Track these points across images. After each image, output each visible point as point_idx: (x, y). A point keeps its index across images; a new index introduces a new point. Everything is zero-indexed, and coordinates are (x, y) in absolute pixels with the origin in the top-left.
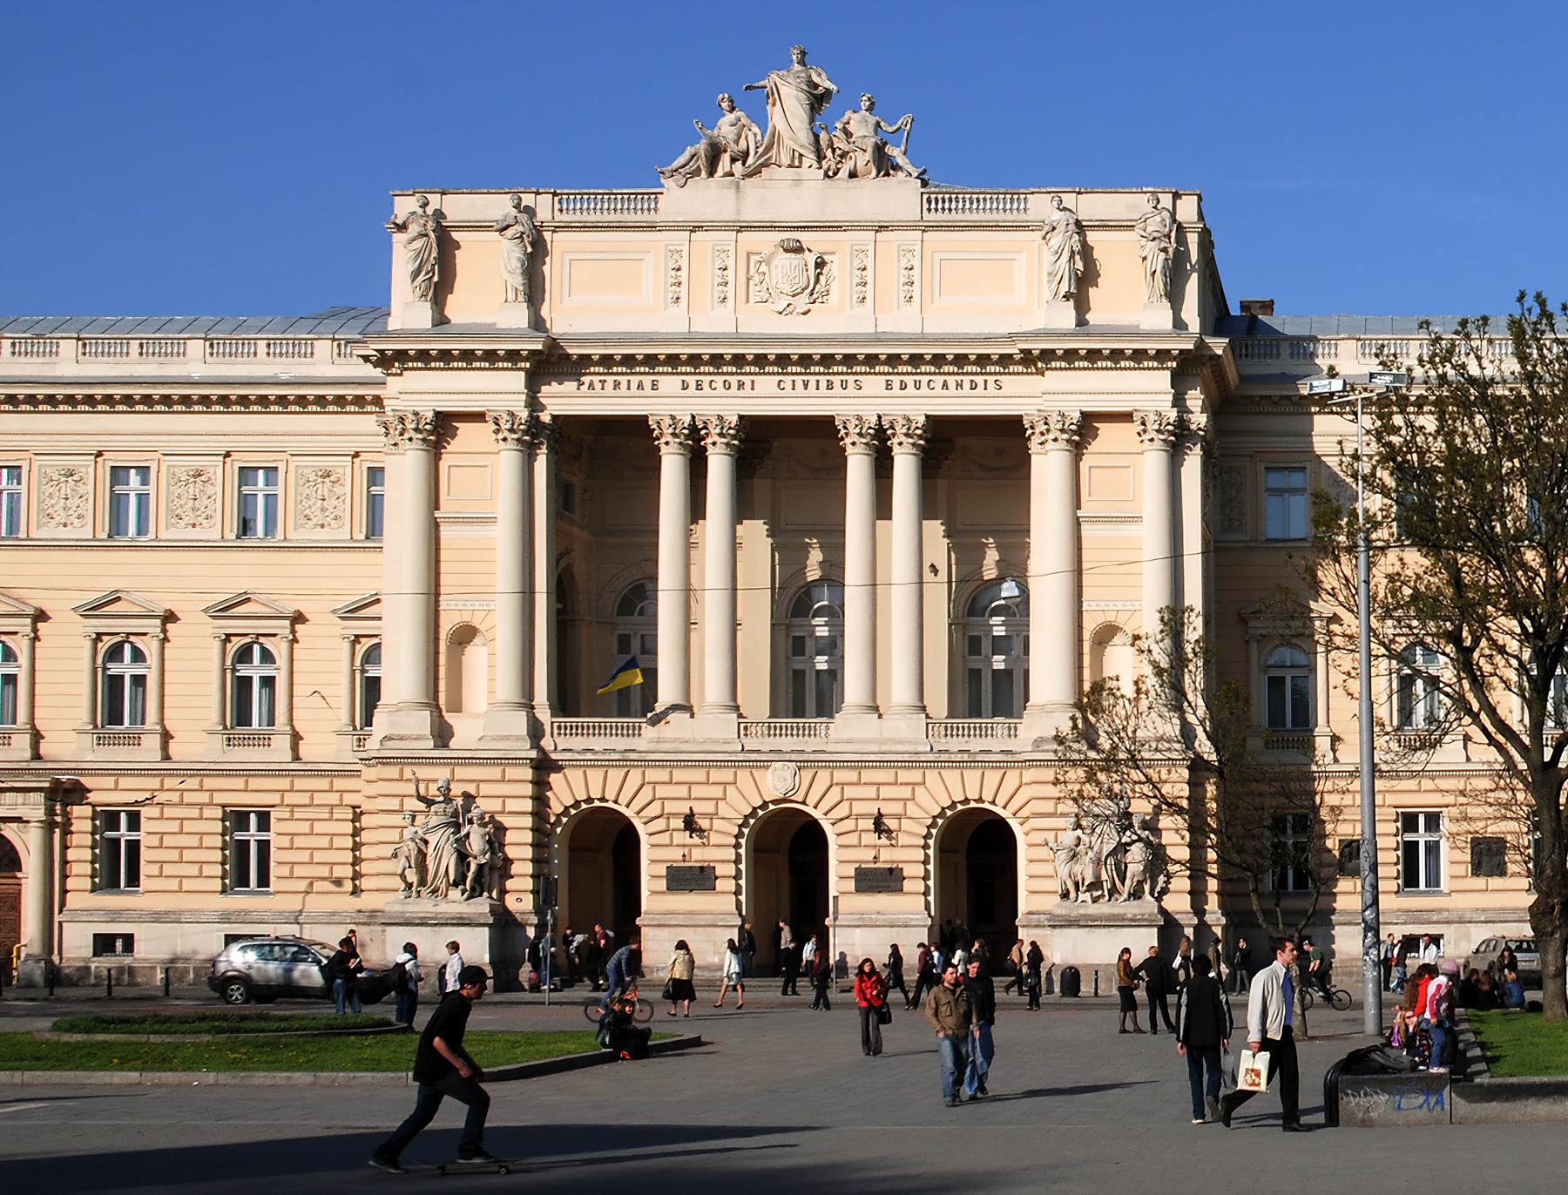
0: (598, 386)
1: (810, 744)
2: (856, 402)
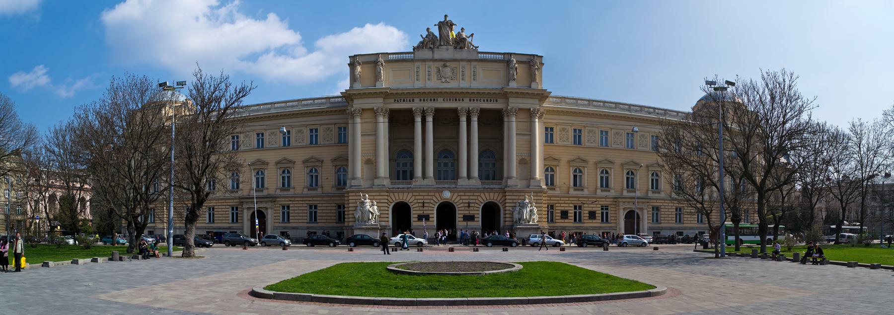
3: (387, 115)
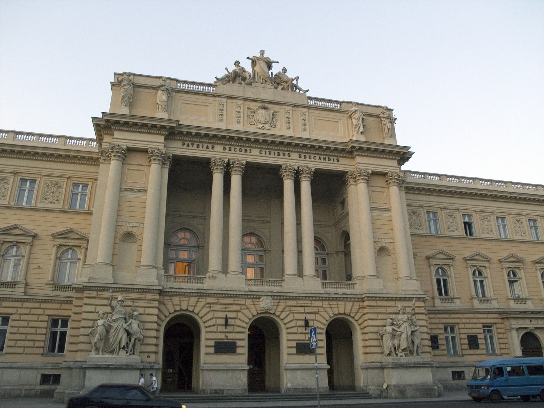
0: (191, 146)
1: (276, 289)
2: (291, 161)
3: (168, 165)
